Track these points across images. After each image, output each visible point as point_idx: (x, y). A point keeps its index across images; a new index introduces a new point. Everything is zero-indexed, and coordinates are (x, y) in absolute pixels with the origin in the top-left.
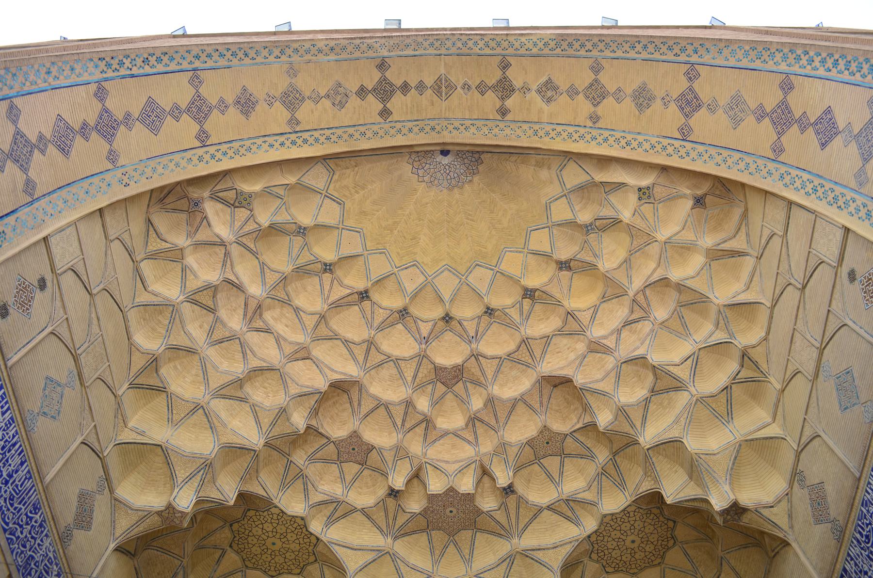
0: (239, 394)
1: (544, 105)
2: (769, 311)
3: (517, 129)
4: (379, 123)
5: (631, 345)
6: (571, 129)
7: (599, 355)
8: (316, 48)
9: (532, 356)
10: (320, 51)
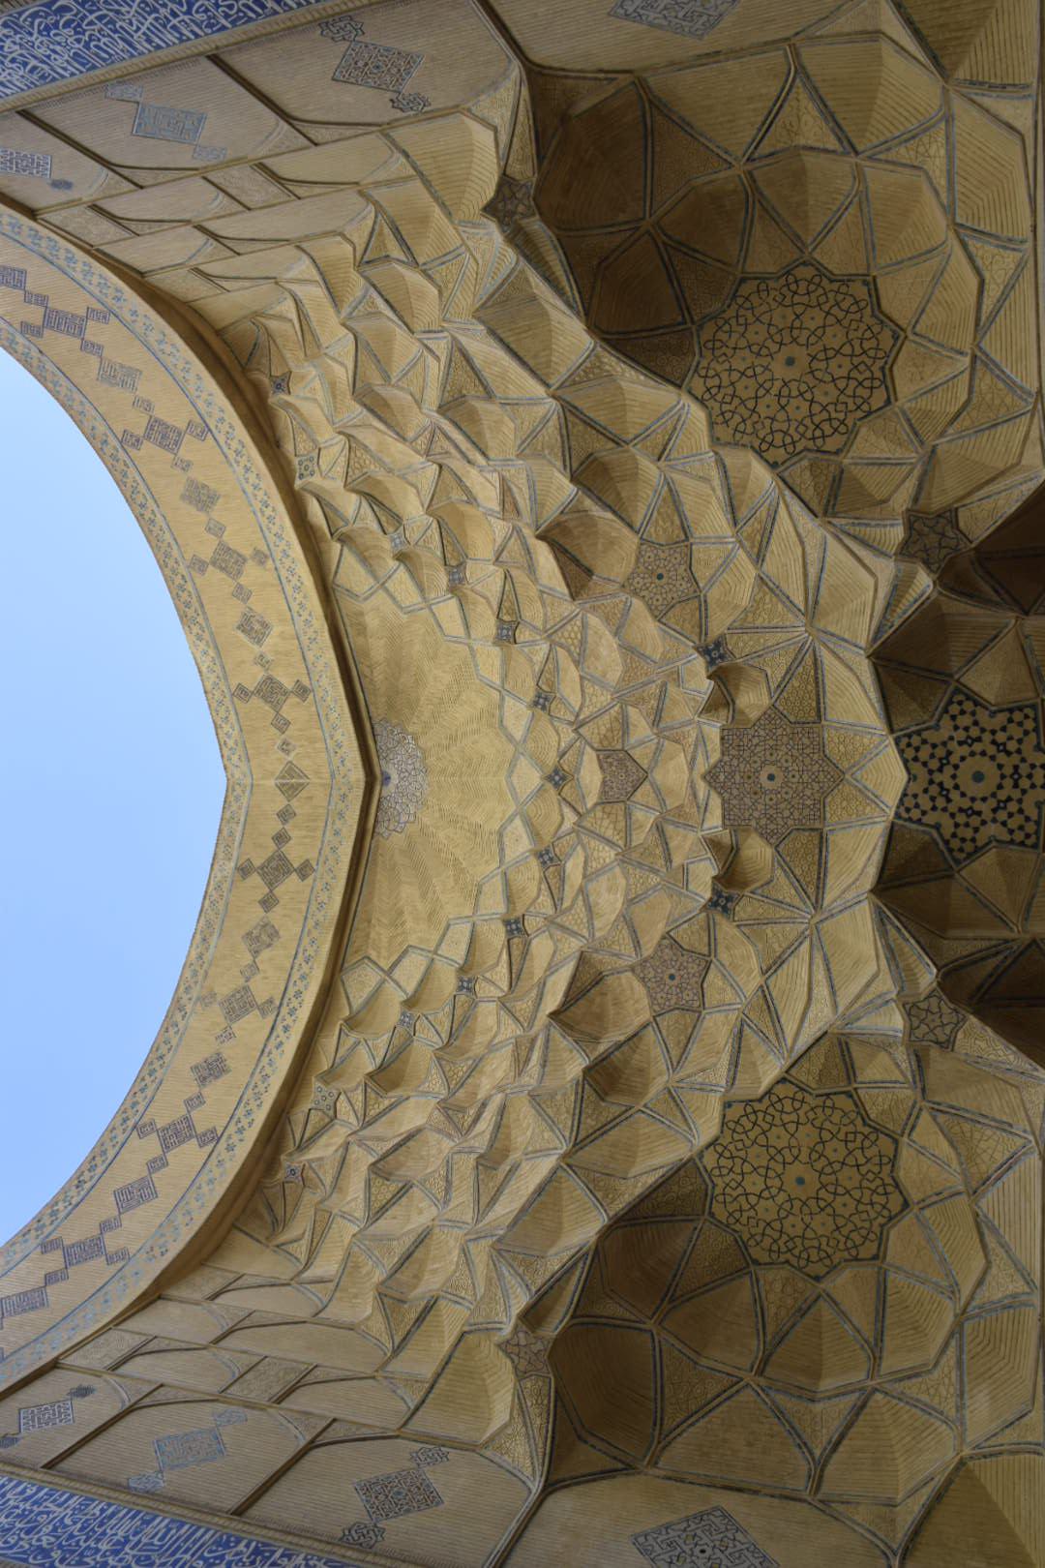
1: (276, 630)
10: (200, 956)
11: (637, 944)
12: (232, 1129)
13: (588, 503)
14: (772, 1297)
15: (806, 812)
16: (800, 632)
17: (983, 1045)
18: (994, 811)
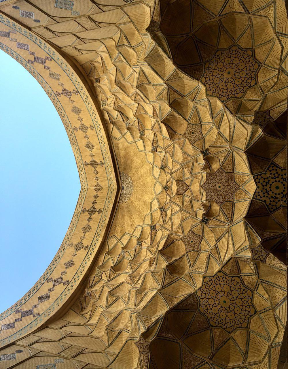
1: (95, 147)
3: (106, 158)
4: (102, 214)
10: (70, 234)
11: (183, 232)
12: (73, 280)
13: (174, 113)
14: (216, 337)
15: (229, 197)
16: (228, 148)
17: (274, 262)
18: (282, 198)
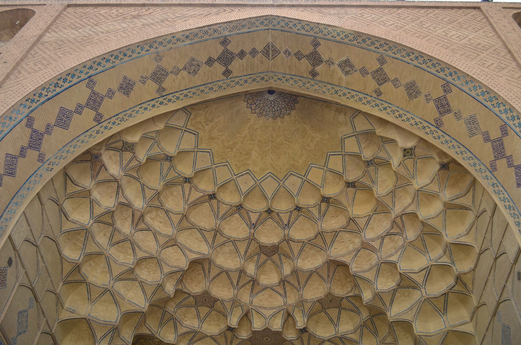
0: (132, 276)
1: (343, 76)
2: (477, 255)
3: (323, 87)
4: (223, 80)
5: (389, 250)
6: (362, 96)
7: (369, 251)
8: (175, 38)
9: (325, 242)
10: (178, 40)
